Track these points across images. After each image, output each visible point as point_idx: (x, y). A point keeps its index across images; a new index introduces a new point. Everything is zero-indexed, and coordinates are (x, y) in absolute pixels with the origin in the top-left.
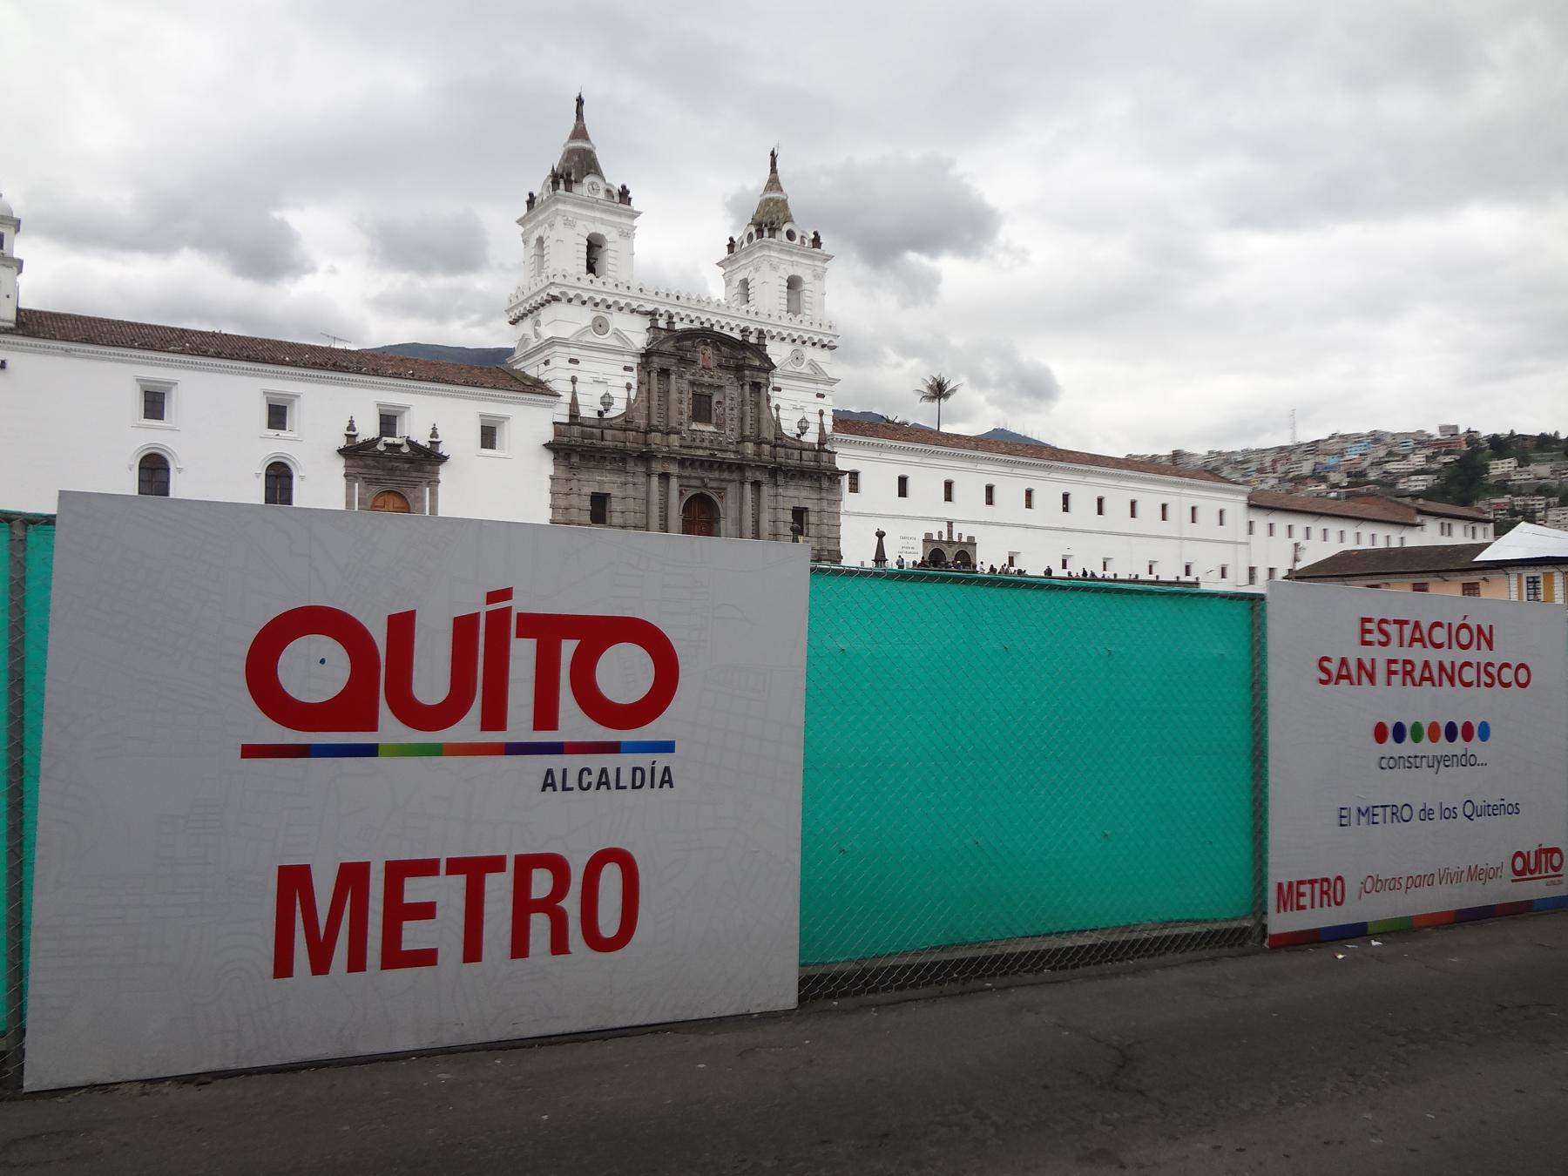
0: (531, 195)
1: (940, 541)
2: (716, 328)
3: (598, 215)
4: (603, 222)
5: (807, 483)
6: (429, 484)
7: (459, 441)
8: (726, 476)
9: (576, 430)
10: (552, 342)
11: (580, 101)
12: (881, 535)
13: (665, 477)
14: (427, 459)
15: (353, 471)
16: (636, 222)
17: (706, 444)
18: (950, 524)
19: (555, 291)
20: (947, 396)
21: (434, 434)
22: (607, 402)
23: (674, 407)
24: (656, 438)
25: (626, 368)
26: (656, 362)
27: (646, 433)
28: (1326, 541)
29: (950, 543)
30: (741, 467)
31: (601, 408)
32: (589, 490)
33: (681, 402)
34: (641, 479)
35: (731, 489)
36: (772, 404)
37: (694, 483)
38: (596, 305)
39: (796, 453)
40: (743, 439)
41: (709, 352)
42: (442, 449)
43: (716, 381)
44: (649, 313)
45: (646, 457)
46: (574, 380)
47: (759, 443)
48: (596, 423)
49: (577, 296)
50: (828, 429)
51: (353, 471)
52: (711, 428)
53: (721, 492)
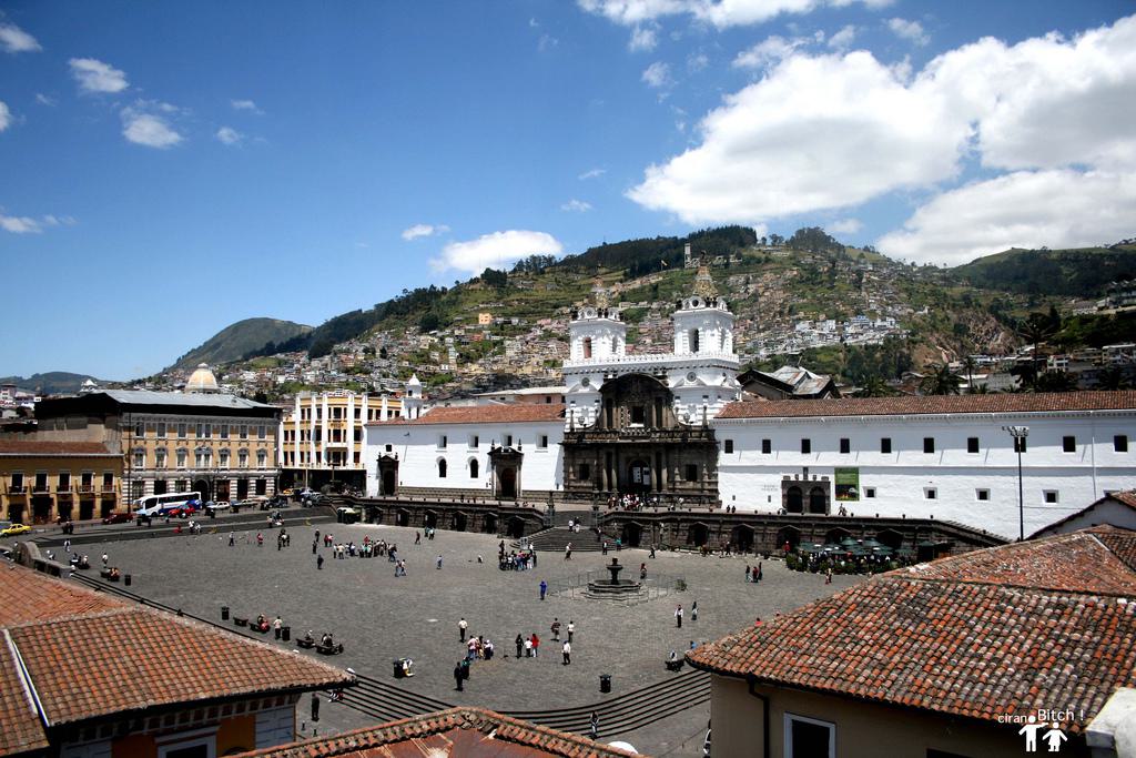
1: (797, 481)
14: (517, 457)
29: (806, 482)
32: (580, 462)
42: (522, 451)
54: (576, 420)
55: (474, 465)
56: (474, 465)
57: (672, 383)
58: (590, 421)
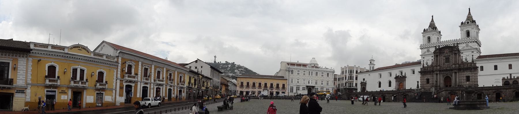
14: (405, 77)
18: (511, 75)
30: (452, 70)
54: (425, 64)
55: (390, 83)
56: (390, 83)
57: (460, 48)
58: (430, 63)
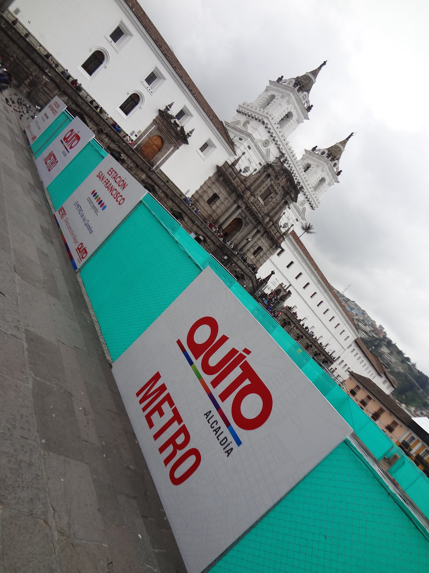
0: (282, 77)
1: (283, 288)
2: (293, 175)
3: (298, 107)
4: (297, 111)
5: (270, 242)
6: (174, 147)
7: (196, 141)
8: (253, 221)
9: (230, 170)
10: (249, 135)
11: (325, 63)
12: (273, 273)
13: (239, 207)
14: (182, 138)
15: (158, 121)
16: (305, 121)
17: (257, 207)
18: (290, 285)
19: (266, 121)
20: (308, 232)
21: (191, 132)
22: (246, 170)
23: (261, 188)
24: (248, 193)
25: (260, 164)
26: (270, 171)
27: (246, 189)
28: (365, 370)
31: (243, 170)
32: (216, 191)
33: (264, 188)
34: (232, 201)
35: (250, 226)
36: (284, 211)
37: (243, 215)
38: (272, 136)
39: (276, 231)
40: (268, 215)
41: (284, 180)
42: (189, 139)
43: (277, 191)
44: (282, 153)
45: (240, 196)
46: (244, 153)
47: (270, 220)
48: (236, 172)
49: (270, 128)
50: (289, 232)
51: (158, 121)
52: (262, 202)
53: (247, 224)
